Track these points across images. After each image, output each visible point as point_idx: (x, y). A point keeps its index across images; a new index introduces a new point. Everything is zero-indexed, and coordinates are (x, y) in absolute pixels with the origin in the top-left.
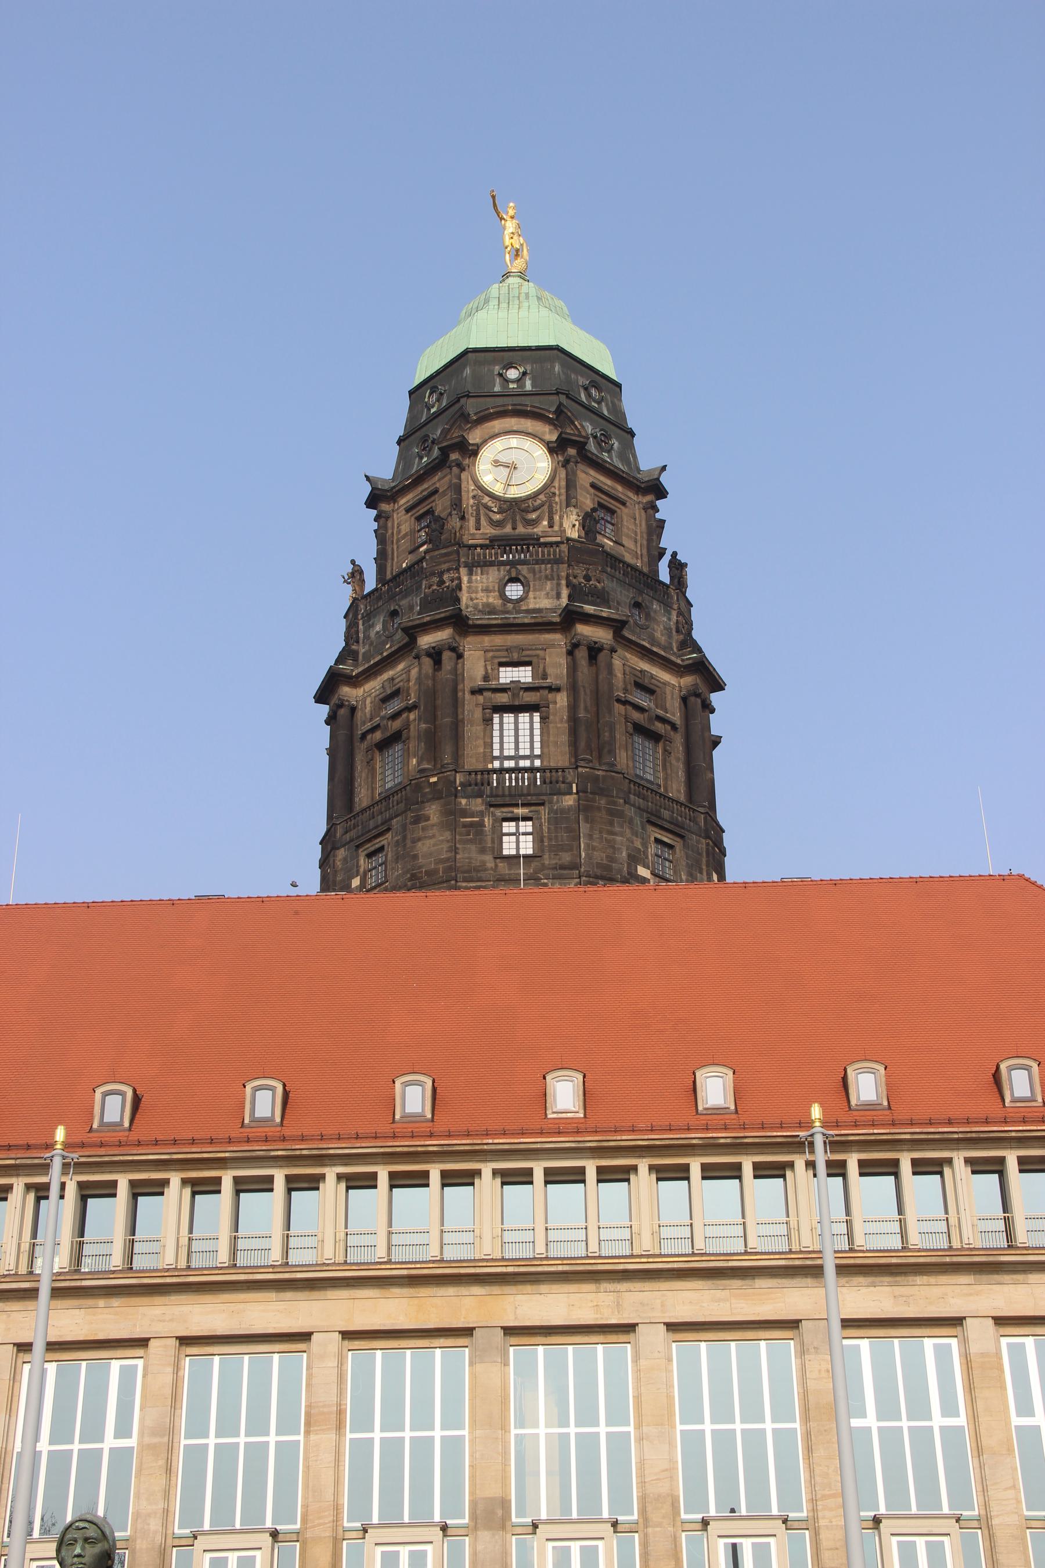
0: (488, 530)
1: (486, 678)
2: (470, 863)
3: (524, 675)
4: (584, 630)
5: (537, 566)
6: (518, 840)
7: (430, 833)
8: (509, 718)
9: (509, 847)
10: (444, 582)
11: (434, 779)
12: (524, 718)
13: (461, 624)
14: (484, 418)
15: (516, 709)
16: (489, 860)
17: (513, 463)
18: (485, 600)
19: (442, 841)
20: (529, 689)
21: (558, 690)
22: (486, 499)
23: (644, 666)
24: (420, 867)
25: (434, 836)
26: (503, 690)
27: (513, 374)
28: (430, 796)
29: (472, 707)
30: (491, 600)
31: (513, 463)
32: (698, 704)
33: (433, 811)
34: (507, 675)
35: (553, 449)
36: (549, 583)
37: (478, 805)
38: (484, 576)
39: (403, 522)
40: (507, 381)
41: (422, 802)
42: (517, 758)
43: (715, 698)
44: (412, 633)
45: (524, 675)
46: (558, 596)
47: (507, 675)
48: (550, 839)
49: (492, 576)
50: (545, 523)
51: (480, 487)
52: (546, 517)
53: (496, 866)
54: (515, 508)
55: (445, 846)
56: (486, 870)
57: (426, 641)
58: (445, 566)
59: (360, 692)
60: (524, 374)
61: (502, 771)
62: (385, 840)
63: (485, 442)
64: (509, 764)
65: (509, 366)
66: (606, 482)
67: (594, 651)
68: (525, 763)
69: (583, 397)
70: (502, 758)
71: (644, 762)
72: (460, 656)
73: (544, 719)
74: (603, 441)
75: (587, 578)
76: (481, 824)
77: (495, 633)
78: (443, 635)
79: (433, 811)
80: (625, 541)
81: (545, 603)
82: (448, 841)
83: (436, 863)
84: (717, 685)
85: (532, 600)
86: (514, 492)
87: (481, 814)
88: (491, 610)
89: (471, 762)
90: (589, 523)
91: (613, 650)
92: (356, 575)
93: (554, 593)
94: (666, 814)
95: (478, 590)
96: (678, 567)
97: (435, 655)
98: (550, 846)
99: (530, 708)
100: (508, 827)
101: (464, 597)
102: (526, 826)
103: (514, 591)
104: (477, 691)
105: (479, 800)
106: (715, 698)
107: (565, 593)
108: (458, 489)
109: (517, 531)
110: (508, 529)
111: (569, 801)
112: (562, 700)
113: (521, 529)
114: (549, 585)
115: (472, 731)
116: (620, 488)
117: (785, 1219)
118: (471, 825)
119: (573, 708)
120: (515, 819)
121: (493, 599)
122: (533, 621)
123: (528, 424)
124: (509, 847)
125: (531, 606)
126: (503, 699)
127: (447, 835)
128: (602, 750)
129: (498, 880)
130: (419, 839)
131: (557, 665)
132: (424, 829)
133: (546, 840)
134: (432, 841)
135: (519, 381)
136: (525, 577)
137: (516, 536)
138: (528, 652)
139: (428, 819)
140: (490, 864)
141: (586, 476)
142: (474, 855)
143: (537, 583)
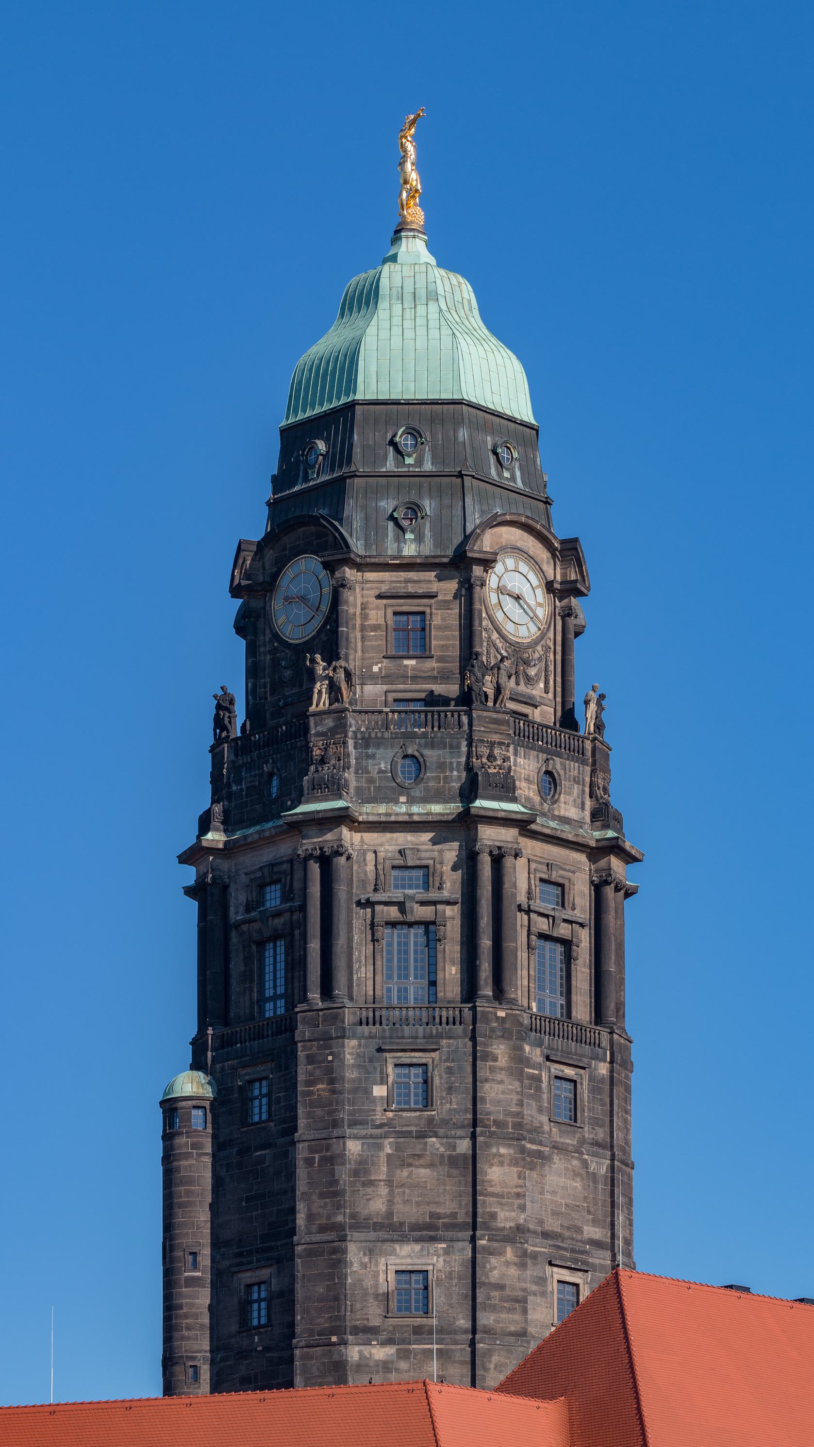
2: (532, 1121)
5: (567, 762)
7: (499, 1077)
10: (495, 759)
11: (501, 1014)
16: (545, 1119)
18: (527, 793)
19: (512, 1091)
22: (495, 636)
24: (488, 1113)
25: (501, 1082)
28: (500, 1034)
30: (531, 794)
36: (576, 786)
38: (526, 761)
41: (490, 1037)
46: (583, 808)
48: (589, 1109)
50: (542, 685)
52: (543, 678)
53: (551, 1130)
55: (515, 1097)
56: (543, 1133)
58: (496, 738)
59: (357, 837)
76: (539, 1079)
77: (537, 839)
81: (572, 813)
82: (517, 1093)
83: (505, 1115)
85: (563, 805)
87: (539, 1067)
93: (580, 801)
98: (590, 1118)
105: (538, 1051)
109: (520, 688)
118: (533, 1077)
122: (574, 839)
125: (562, 813)
127: (517, 1084)
129: (554, 1147)
130: (487, 1080)
132: (492, 1069)
133: (586, 1109)
134: (501, 1087)
136: (558, 773)
138: (562, 872)
139: (495, 1059)
140: (546, 1128)
142: (534, 1113)
143: (567, 783)
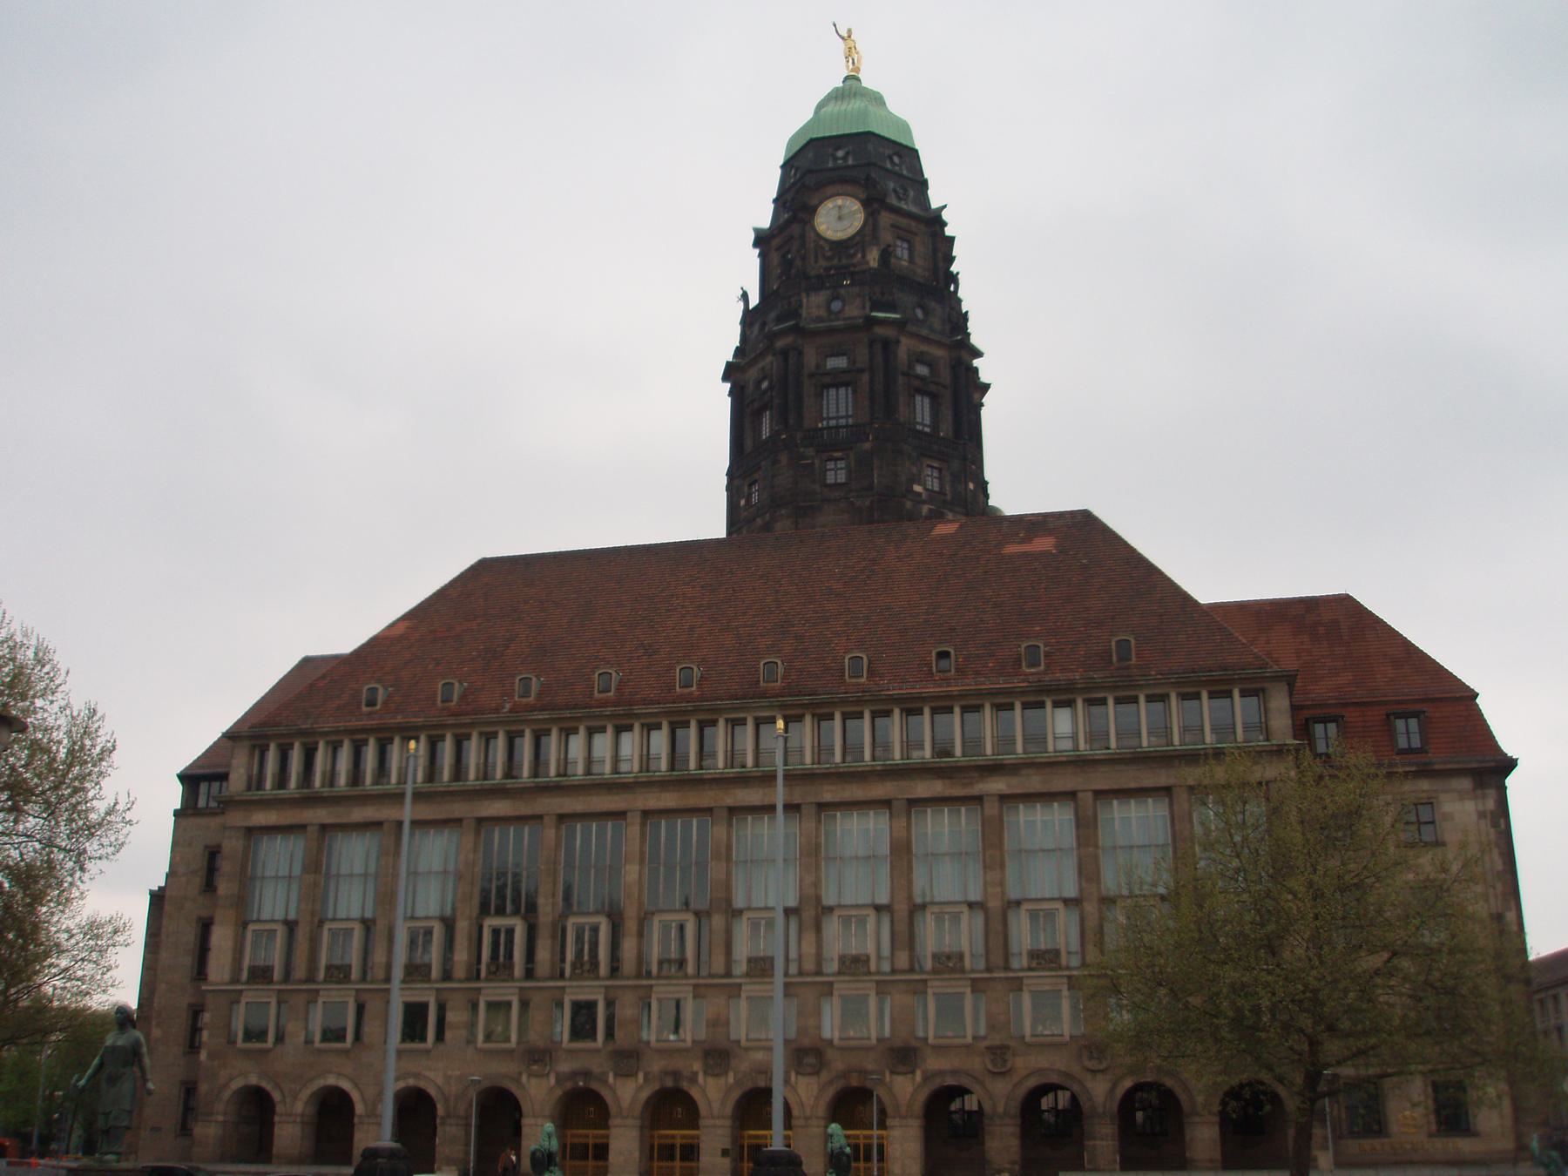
0: (822, 263)
1: (818, 366)
3: (840, 363)
4: (879, 331)
6: (837, 474)
8: (833, 392)
9: (830, 479)
12: (842, 391)
14: (820, 186)
15: (837, 386)
17: (838, 218)
20: (844, 371)
21: (862, 371)
23: (924, 348)
26: (828, 374)
27: (840, 153)
33: (784, 459)
35: (866, 204)
37: (811, 452)
40: (836, 159)
42: (838, 418)
43: (976, 362)
45: (840, 363)
51: (818, 234)
54: (840, 246)
57: (780, 343)
60: (847, 154)
61: (829, 428)
62: (756, 476)
63: (821, 202)
64: (833, 423)
65: (838, 148)
66: (903, 222)
68: (843, 422)
69: (889, 166)
70: (829, 419)
72: (801, 353)
73: (854, 391)
75: (883, 294)
79: (784, 459)
80: (920, 261)
84: (978, 354)
86: (840, 236)
88: (820, 319)
89: (807, 424)
91: (898, 342)
92: (745, 297)
94: (935, 447)
97: (785, 353)
99: (846, 385)
100: (831, 465)
101: (804, 312)
102: (841, 464)
103: (836, 306)
104: (812, 376)
106: (976, 362)
107: (868, 305)
108: (803, 236)
110: (836, 261)
111: (867, 446)
112: (865, 378)
113: (844, 261)
114: (858, 301)
116: (913, 224)
117: (634, 829)
119: (872, 380)
120: (836, 459)
121: (823, 313)
123: (849, 189)
124: (830, 479)
126: (827, 380)
131: (862, 355)
135: (845, 158)
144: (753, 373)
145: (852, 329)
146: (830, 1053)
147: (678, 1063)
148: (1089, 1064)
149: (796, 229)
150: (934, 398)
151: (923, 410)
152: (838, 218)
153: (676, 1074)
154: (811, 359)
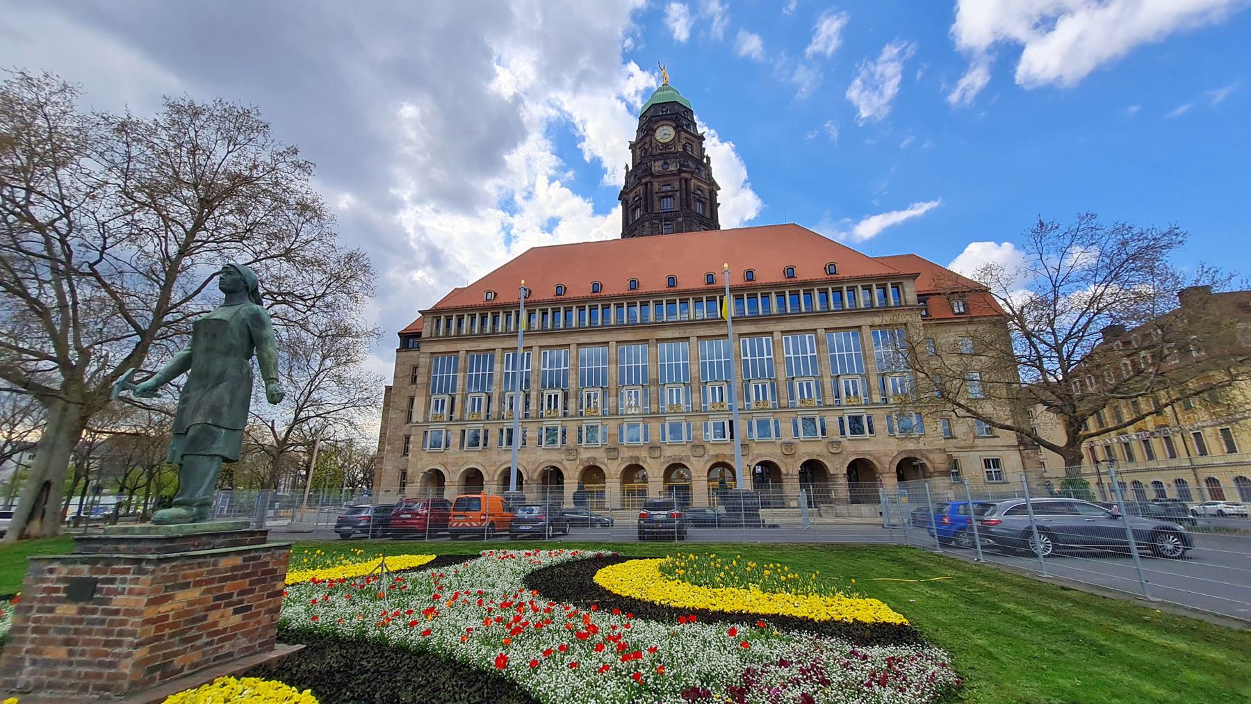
3: (669, 188)
13: (652, 175)
29: (656, 197)
31: (665, 134)
32: (713, 194)
33: (647, 224)
34: (664, 189)
39: (638, 152)
44: (640, 179)
45: (669, 188)
47: (664, 189)
49: (661, 162)
67: (686, 180)
71: (699, 208)
74: (688, 126)
78: (647, 179)
90: (684, 147)
95: (657, 167)
96: (708, 159)
97: (646, 184)
115: (656, 203)
128: (688, 206)
131: (676, 185)
137: (666, 153)
141: (683, 134)
144: (632, 195)
145: (673, 174)
146: (708, 446)
147: (636, 453)
148: (833, 451)
149: (647, 139)
150: (703, 203)
151: (699, 208)
152: (665, 134)
153: (638, 458)
154: (656, 187)
